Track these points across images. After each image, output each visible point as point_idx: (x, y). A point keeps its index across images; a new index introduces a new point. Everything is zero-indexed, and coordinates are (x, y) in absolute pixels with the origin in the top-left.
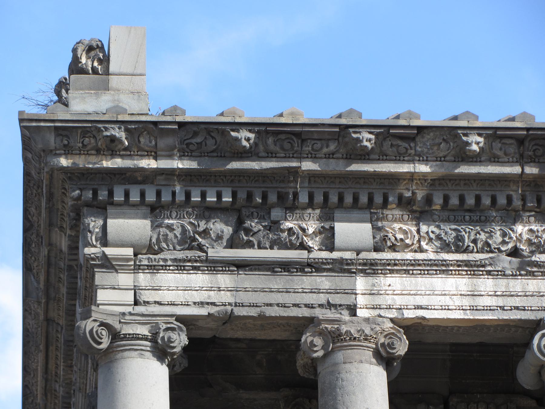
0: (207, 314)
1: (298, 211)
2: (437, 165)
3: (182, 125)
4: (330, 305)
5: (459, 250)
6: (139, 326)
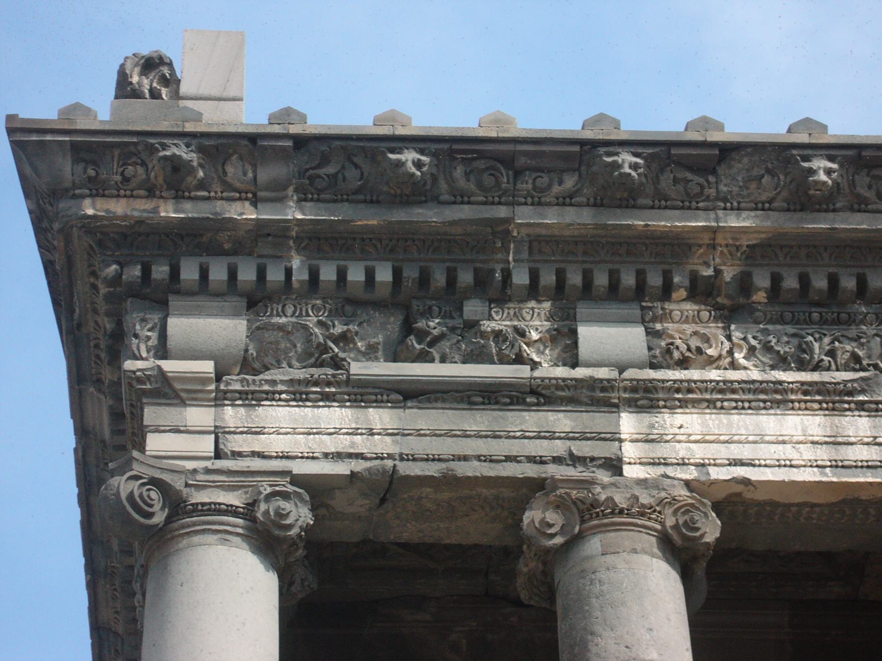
0: (348, 473)
1: (511, 305)
2: (756, 216)
3: (301, 142)
4: (575, 460)
5: (802, 366)
6: (222, 493)
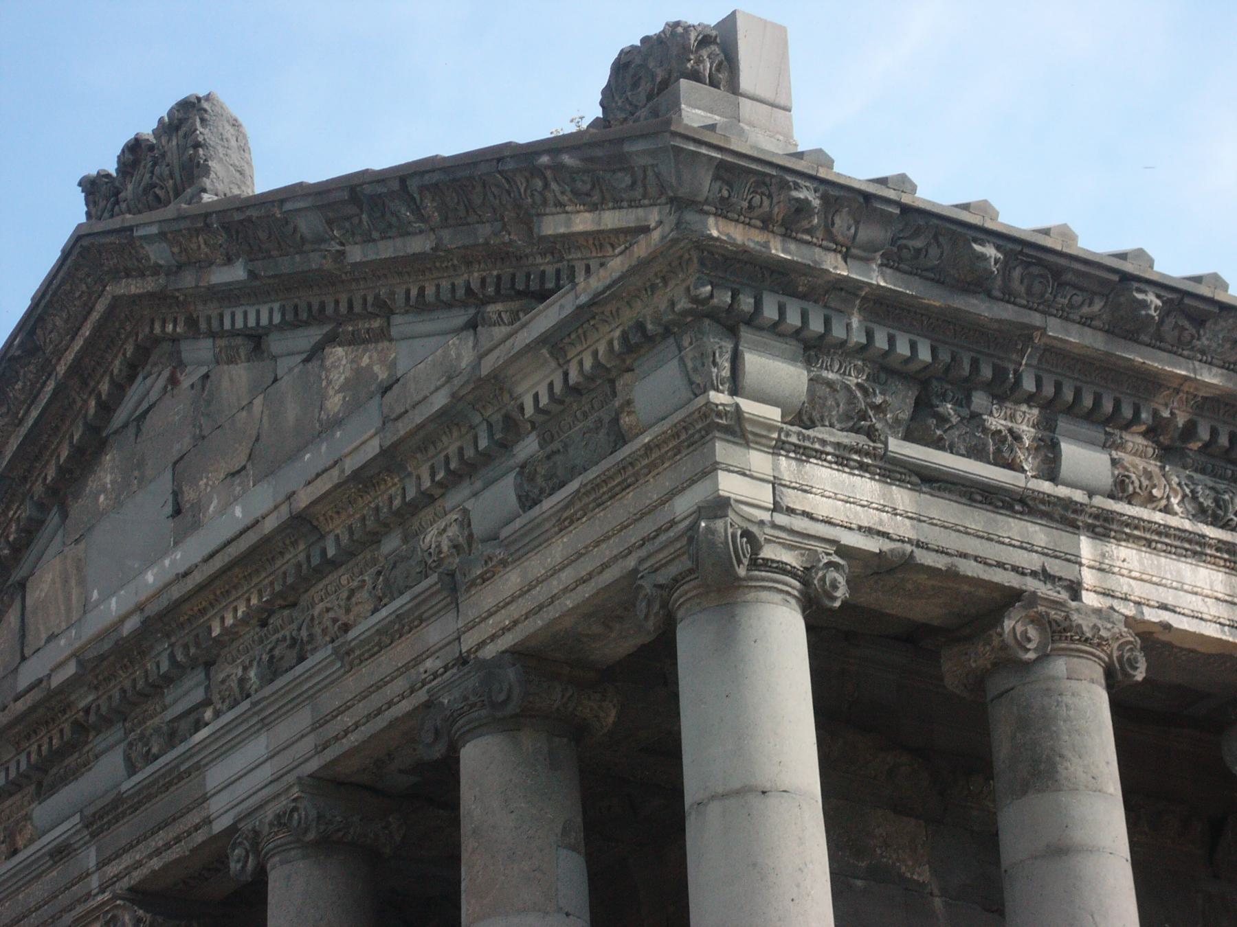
1: (1008, 404)
2: (1222, 375)
6: (784, 551)
